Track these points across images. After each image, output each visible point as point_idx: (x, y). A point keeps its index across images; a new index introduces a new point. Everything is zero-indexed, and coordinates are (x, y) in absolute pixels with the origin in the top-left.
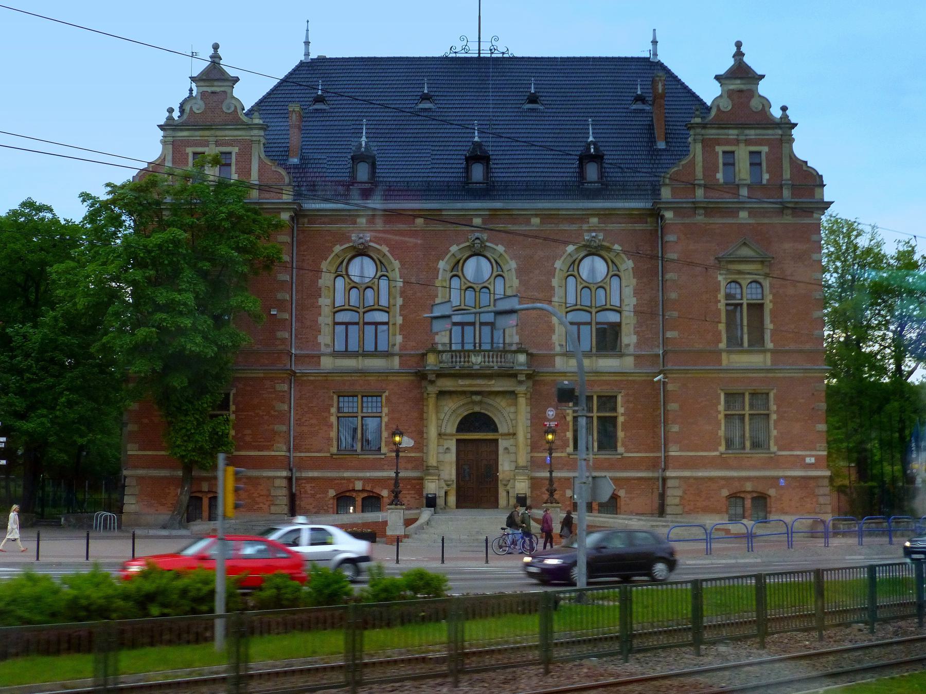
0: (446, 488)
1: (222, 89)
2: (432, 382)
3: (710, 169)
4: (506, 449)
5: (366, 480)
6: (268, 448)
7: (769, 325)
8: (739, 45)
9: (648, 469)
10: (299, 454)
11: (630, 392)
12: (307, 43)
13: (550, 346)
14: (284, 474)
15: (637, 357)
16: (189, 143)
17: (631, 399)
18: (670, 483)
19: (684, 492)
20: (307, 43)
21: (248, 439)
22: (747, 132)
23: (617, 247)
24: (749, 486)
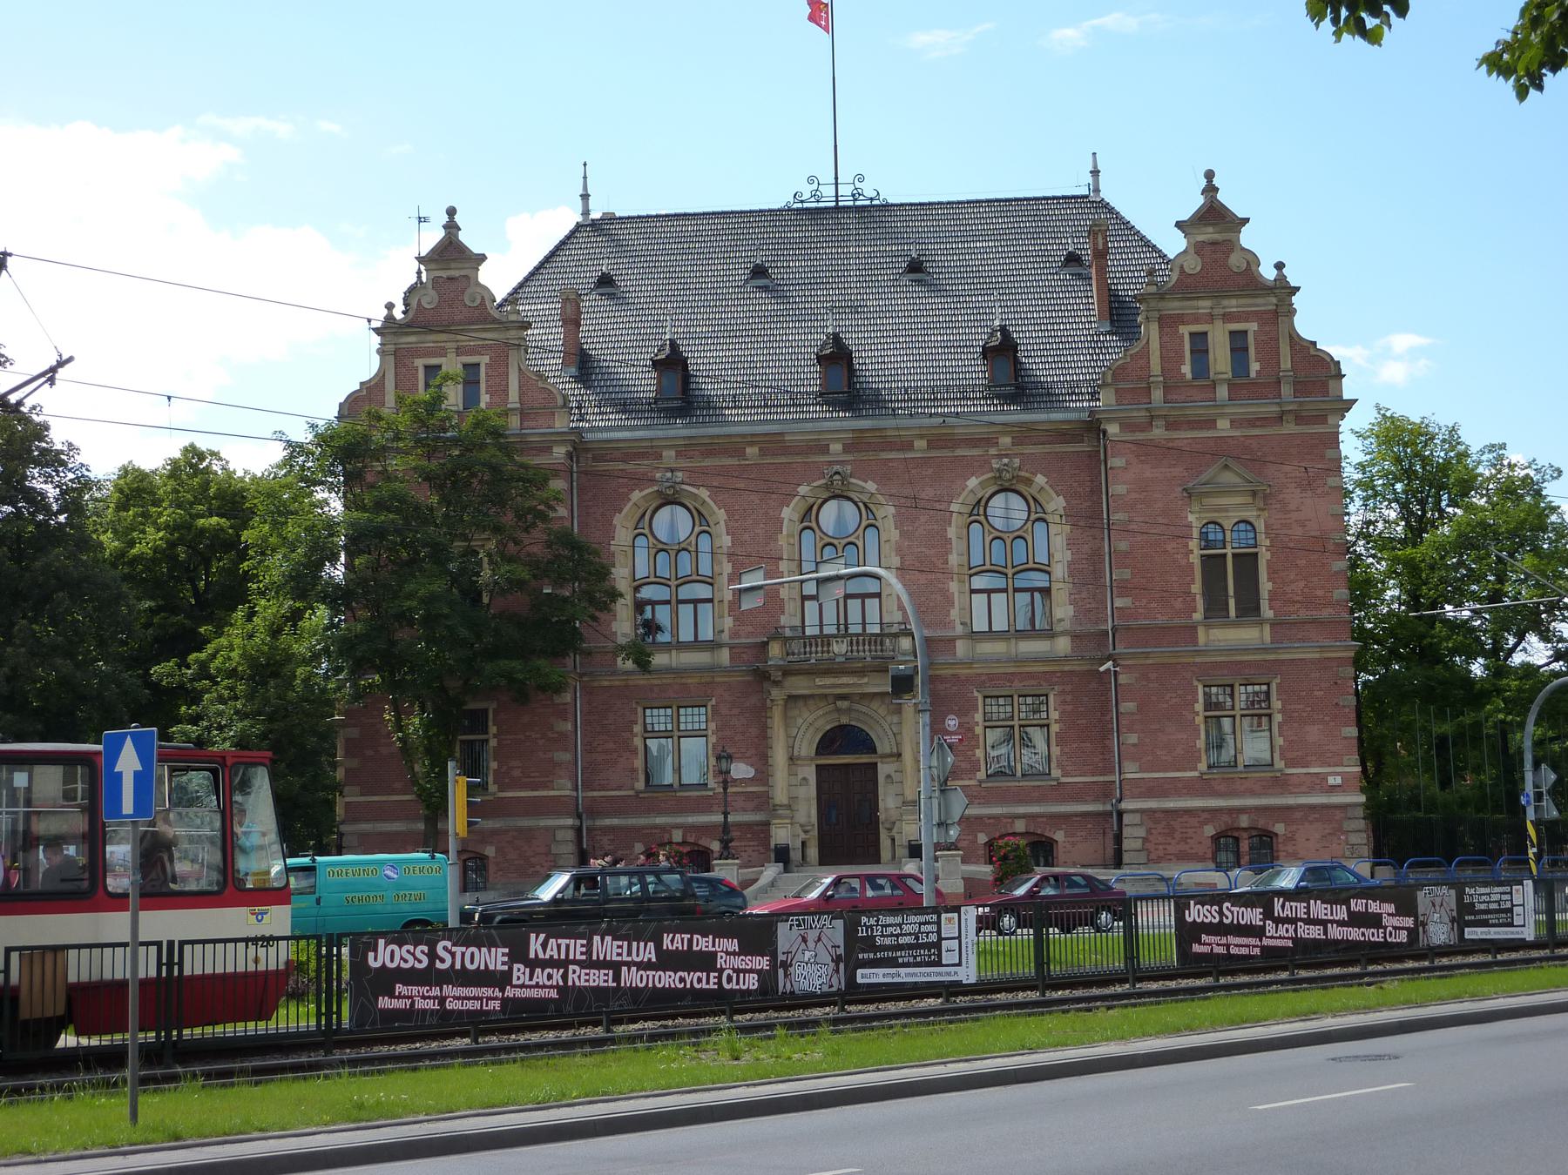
0: (803, 836)
1: (463, 273)
2: (777, 683)
3: (1170, 359)
4: (889, 776)
5: (687, 829)
6: (545, 786)
7: (1265, 586)
8: (1210, 175)
9: (1096, 800)
10: (590, 794)
11: (1068, 688)
12: (585, 197)
13: (949, 625)
14: (570, 822)
15: (1075, 637)
16: (416, 352)
17: (1069, 698)
18: (1126, 819)
19: (1149, 831)
20: (585, 197)
21: (516, 773)
22: (1226, 302)
23: (1040, 479)
24: (1244, 821)
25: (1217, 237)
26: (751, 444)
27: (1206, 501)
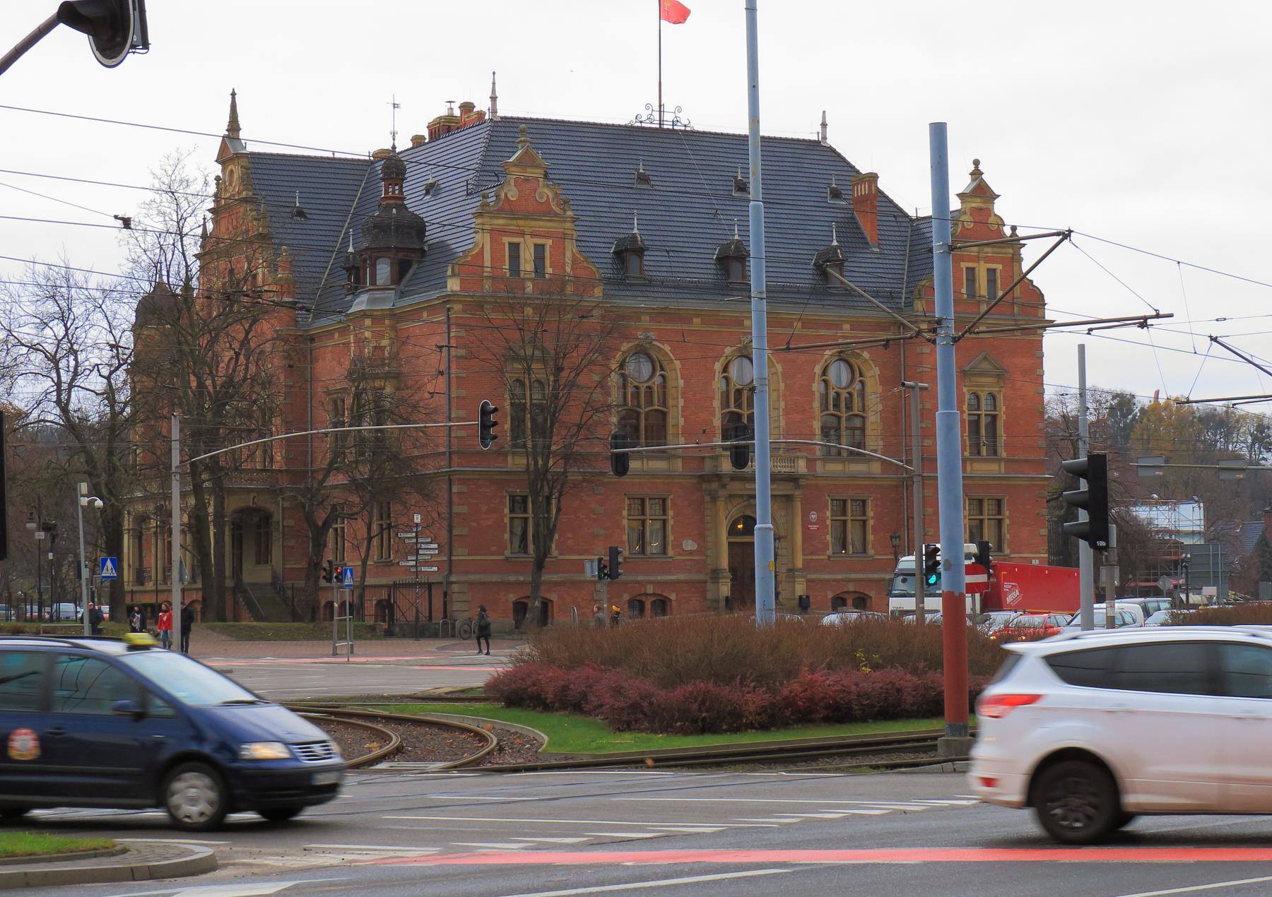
8: (976, 163)
21: (570, 542)
23: (866, 355)
25: (981, 205)
26: (698, 316)
27: (974, 379)
